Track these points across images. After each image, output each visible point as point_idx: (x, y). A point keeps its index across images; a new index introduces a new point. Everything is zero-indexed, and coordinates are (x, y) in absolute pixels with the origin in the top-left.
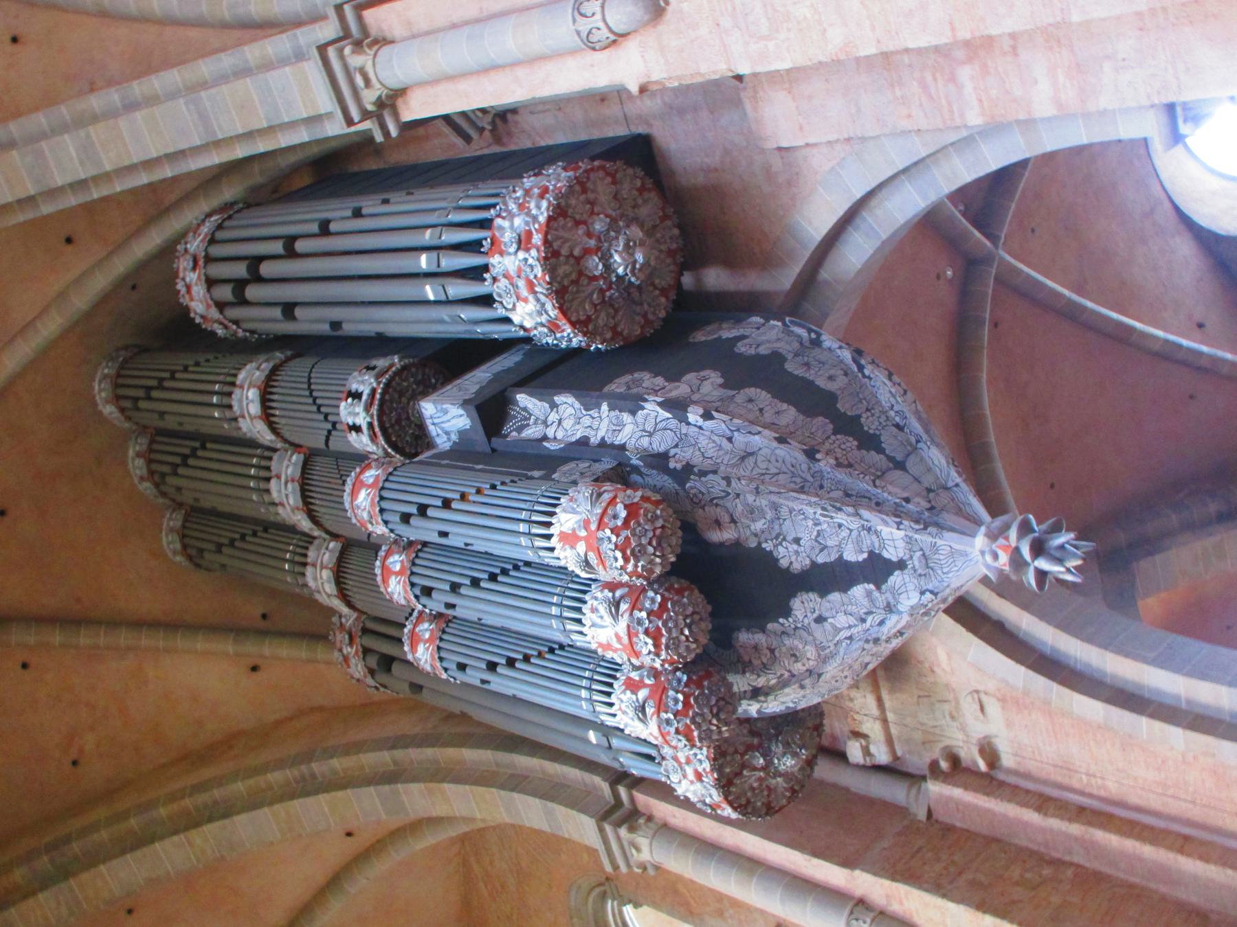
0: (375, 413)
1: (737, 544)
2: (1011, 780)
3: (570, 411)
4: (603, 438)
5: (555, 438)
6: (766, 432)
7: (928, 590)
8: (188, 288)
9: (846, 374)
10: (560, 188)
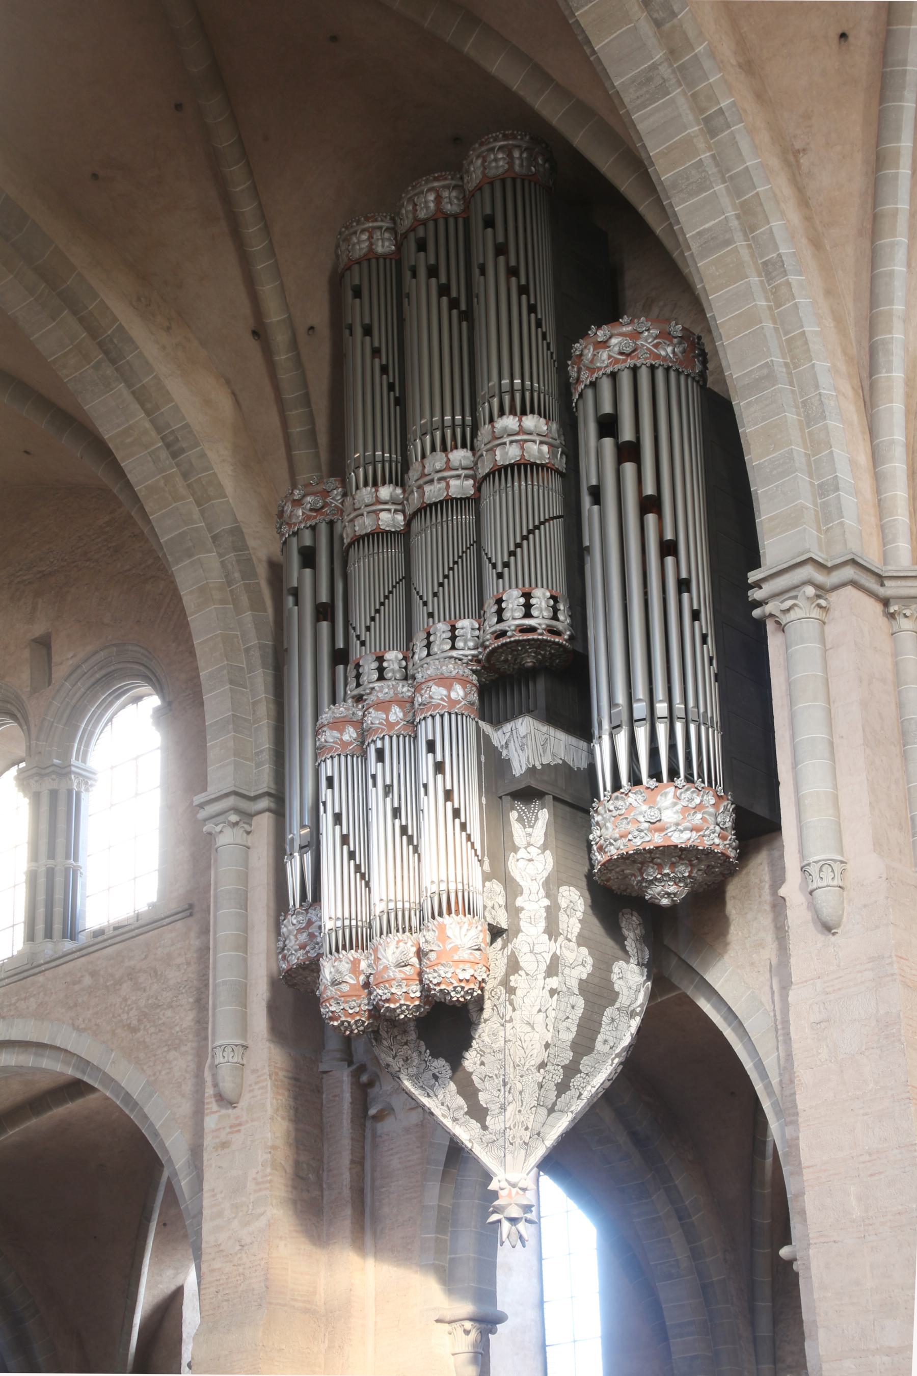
0: (517, 638)
3: (541, 867)
4: (522, 909)
5: (518, 860)
7: (473, 1143)
9: (611, 1048)
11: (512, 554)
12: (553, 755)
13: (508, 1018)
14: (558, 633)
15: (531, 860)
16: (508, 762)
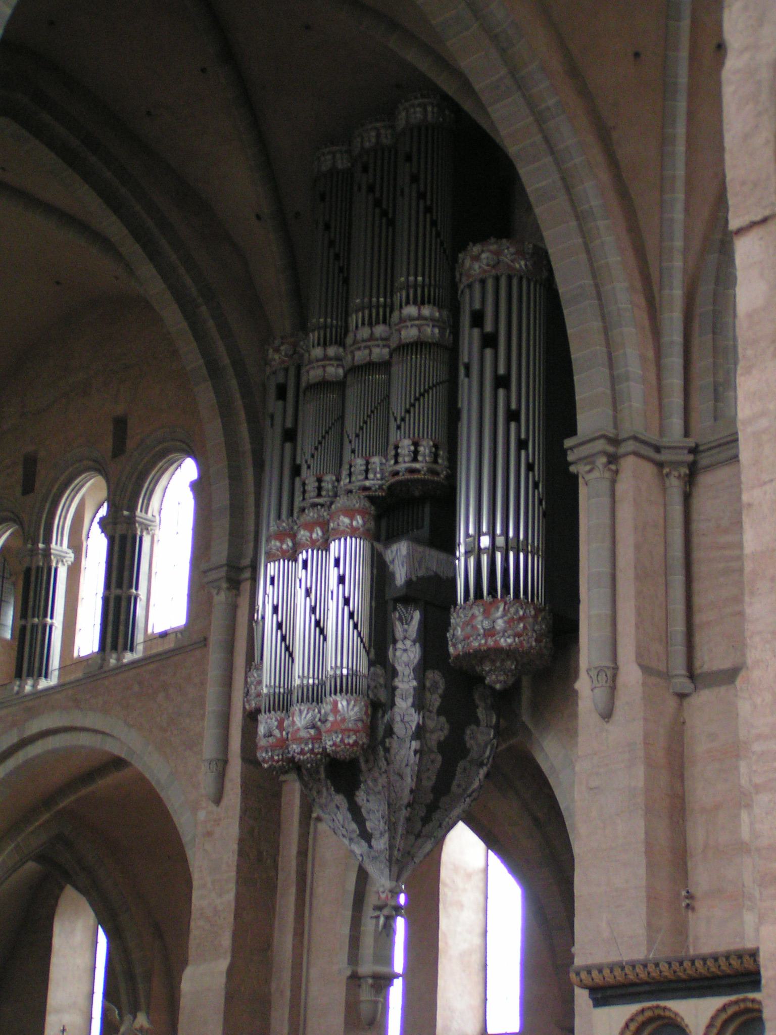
1: (360, 771)
2: (312, 830)
3: (412, 656)
6: (414, 784)
8: (477, 258)
10: (522, 646)
11: (408, 411)
12: (427, 569)
13: (383, 770)
14: (438, 474)
15: (405, 650)
16: (392, 576)
